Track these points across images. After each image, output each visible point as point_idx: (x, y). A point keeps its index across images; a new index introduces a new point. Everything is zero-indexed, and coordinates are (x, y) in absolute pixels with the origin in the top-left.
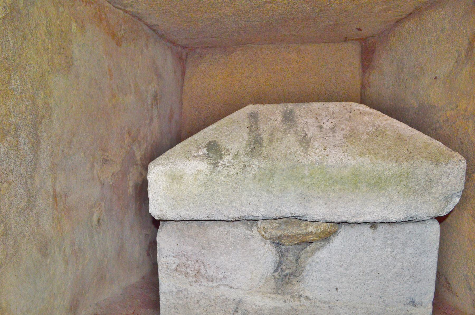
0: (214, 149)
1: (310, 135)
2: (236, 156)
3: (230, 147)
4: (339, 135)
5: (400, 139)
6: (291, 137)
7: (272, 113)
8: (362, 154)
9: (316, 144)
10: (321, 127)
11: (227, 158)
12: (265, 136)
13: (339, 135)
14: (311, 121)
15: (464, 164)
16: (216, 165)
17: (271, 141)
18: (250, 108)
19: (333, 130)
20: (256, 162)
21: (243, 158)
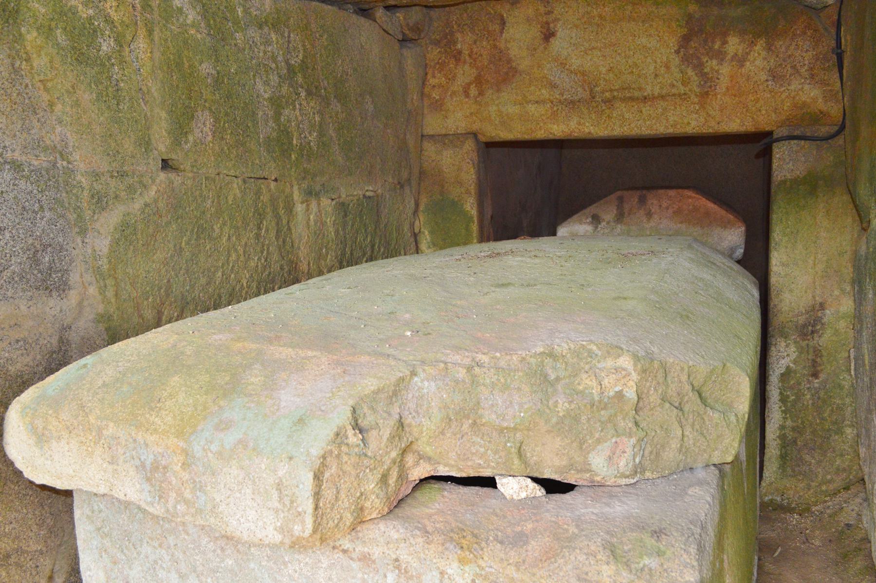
0: (596, 220)
1: (653, 210)
2: (608, 223)
3: (605, 217)
4: (670, 211)
5: (707, 214)
6: (642, 212)
7: (633, 198)
8: (681, 222)
9: (656, 216)
10: (660, 206)
11: (603, 224)
12: (626, 211)
13: (670, 211)
14: (655, 202)
15: (743, 229)
16: (596, 227)
17: (629, 214)
18: (619, 193)
19: (667, 208)
20: (619, 226)
21: (612, 224)
